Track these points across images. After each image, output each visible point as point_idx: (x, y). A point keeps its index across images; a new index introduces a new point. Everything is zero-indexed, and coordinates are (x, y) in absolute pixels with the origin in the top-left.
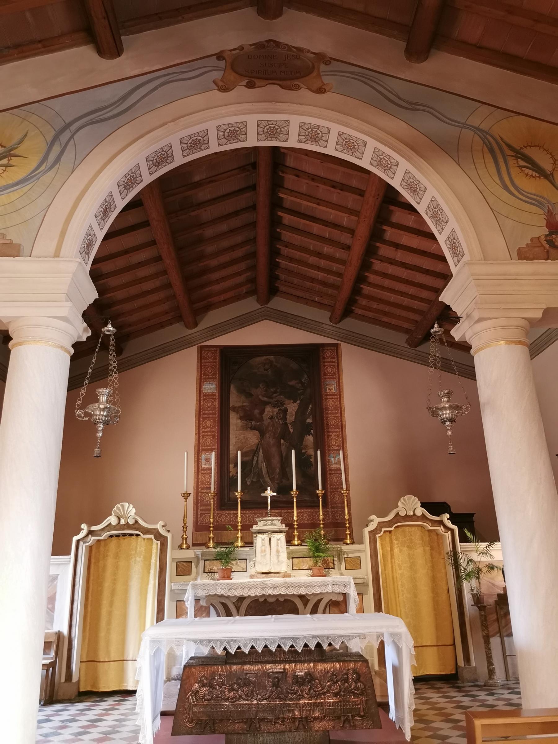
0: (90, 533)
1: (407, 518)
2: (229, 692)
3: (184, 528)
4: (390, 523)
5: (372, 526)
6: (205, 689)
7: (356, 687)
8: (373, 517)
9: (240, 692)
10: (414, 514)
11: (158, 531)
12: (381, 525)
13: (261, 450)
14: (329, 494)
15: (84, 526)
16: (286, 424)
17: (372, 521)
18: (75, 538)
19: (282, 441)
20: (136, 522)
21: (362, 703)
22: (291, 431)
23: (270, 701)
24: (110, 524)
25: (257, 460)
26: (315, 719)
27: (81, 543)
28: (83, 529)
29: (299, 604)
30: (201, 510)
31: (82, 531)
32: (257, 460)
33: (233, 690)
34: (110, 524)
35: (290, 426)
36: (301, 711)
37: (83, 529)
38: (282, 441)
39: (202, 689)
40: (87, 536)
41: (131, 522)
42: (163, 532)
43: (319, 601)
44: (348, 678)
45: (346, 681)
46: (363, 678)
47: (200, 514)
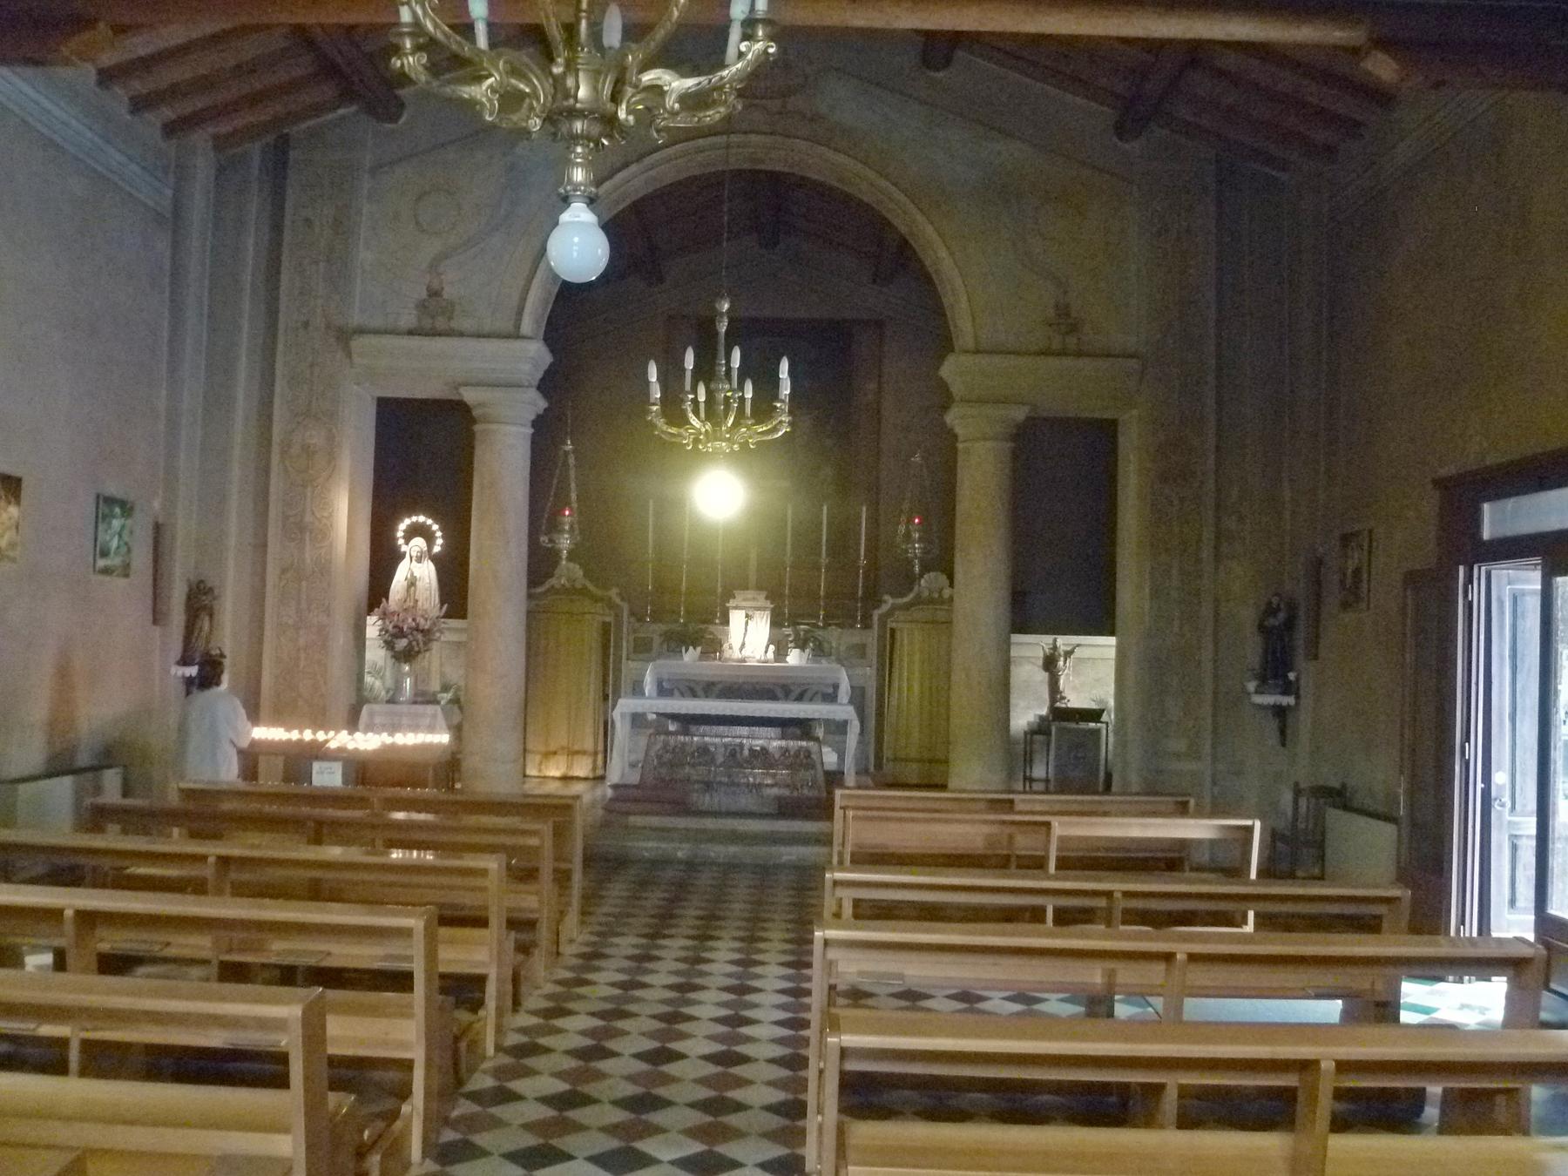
1: (931, 601)
4: (907, 607)
5: (885, 608)
8: (886, 597)
10: (940, 596)
12: (894, 608)
17: (885, 602)
20: (585, 588)
24: (553, 587)
26: (767, 785)
29: (779, 692)
34: (553, 587)
36: (754, 778)
41: (578, 586)
42: (618, 601)
43: (805, 691)
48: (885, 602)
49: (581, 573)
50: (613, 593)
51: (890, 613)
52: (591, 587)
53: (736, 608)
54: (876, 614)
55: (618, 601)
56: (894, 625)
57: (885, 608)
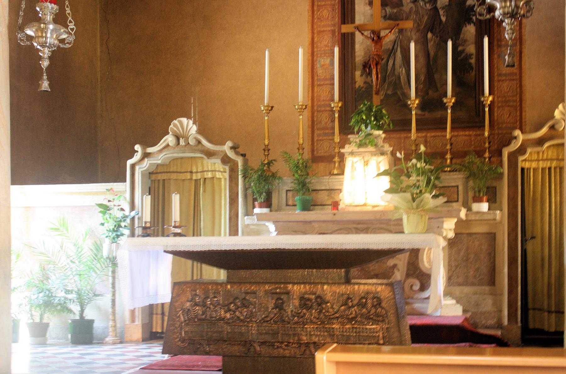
0: (146, 155)
2: (226, 312)
3: (265, 152)
4: (540, 142)
5: (515, 146)
6: (197, 308)
7: (375, 312)
8: (517, 133)
9: (237, 313)
11: (226, 154)
13: (399, 49)
14: (496, 109)
15: (137, 147)
16: (435, 9)
18: (129, 162)
19: (430, 35)
20: (199, 142)
21: (382, 330)
22: (443, 19)
23: (272, 324)
24: (168, 145)
25: (394, 64)
27: (137, 168)
28: (137, 152)
30: (319, 135)
31: (136, 154)
32: (394, 64)
33: (229, 310)
34: (168, 145)
35: (441, 12)
37: (137, 152)
38: (430, 35)
39: (194, 308)
40: (142, 159)
42: (231, 154)
44: (366, 303)
45: (364, 305)
46: (386, 304)
47: (317, 140)
48: (515, 138)
49: (194, 128)
50: (227, 147)
51: (522, 150)
52: (205, 142)
53: (352, 153)
54: (506, 152)
55: (231, 154)
56: (527, 165)
57: (515, 146)
